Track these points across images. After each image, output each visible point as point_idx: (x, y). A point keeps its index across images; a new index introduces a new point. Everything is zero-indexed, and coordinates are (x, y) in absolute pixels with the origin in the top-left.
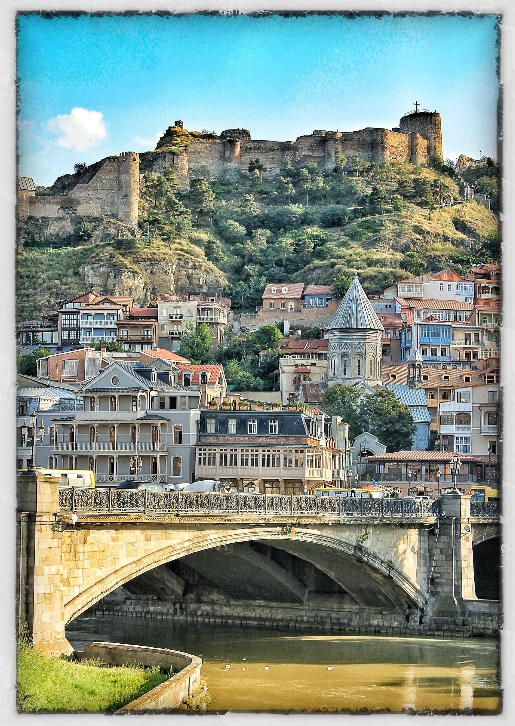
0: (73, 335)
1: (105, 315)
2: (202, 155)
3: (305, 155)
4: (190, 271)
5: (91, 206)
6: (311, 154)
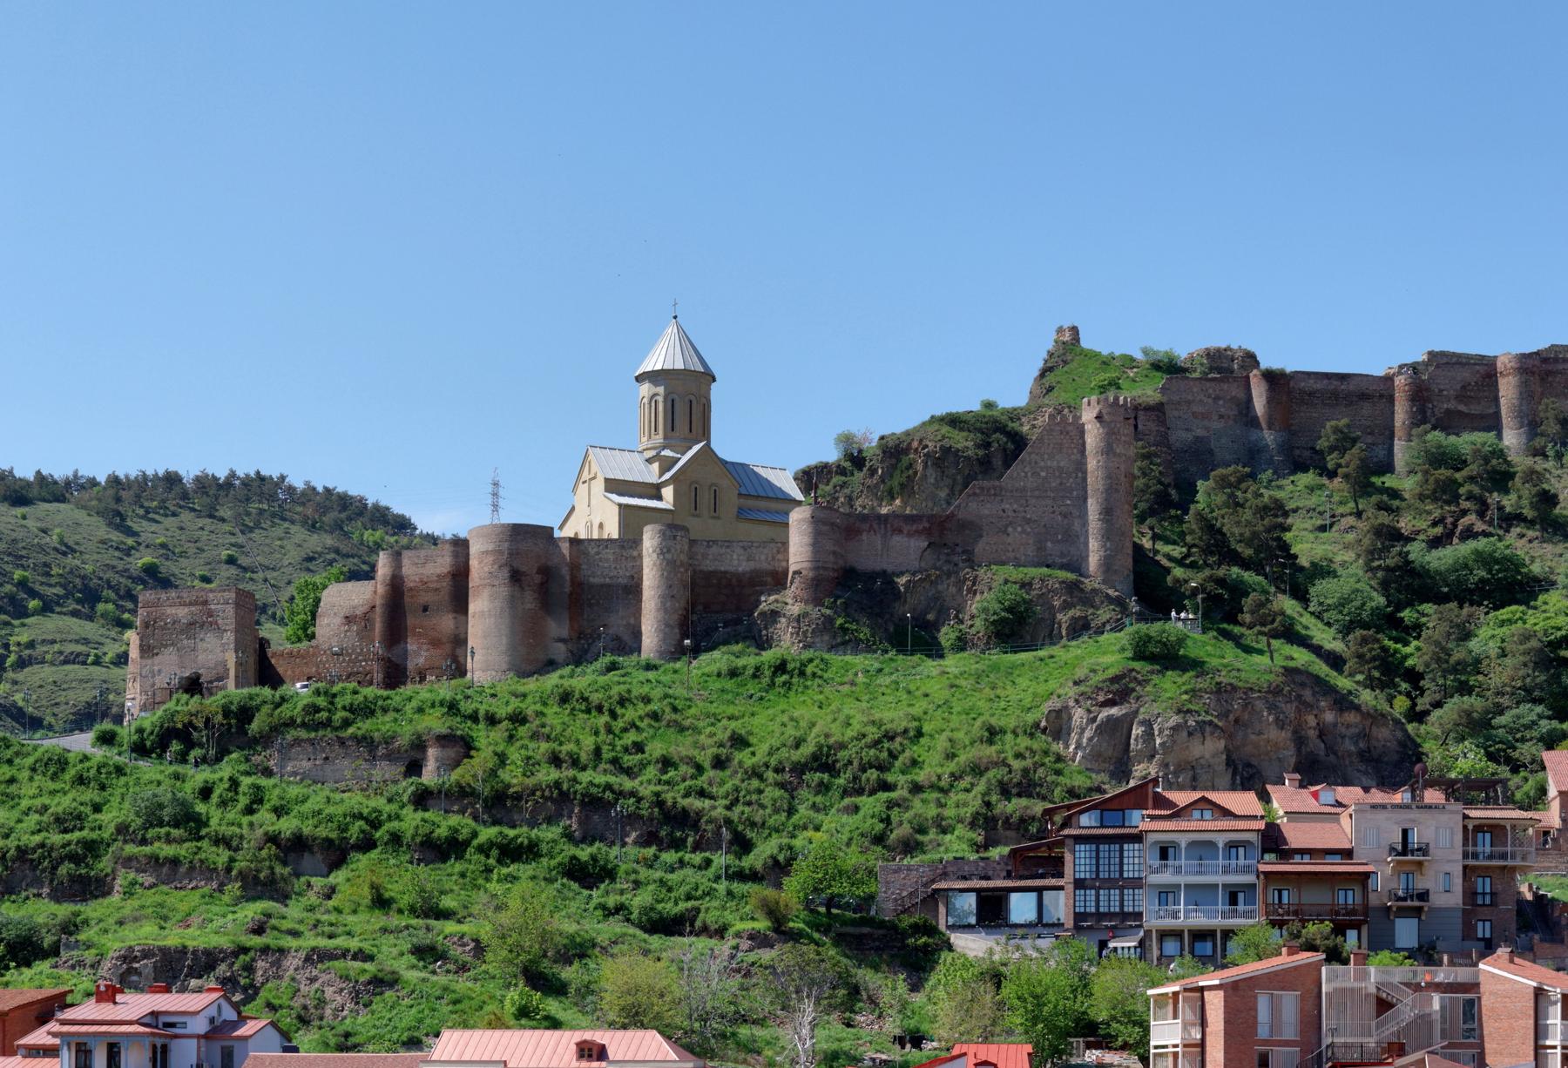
0: (1110, 901)
1: (1221, 845)
2: (1195, 409)
3: (1448, 411)
4: (1329, 717)
5: (1009, 540)
6: (1462, 408)
